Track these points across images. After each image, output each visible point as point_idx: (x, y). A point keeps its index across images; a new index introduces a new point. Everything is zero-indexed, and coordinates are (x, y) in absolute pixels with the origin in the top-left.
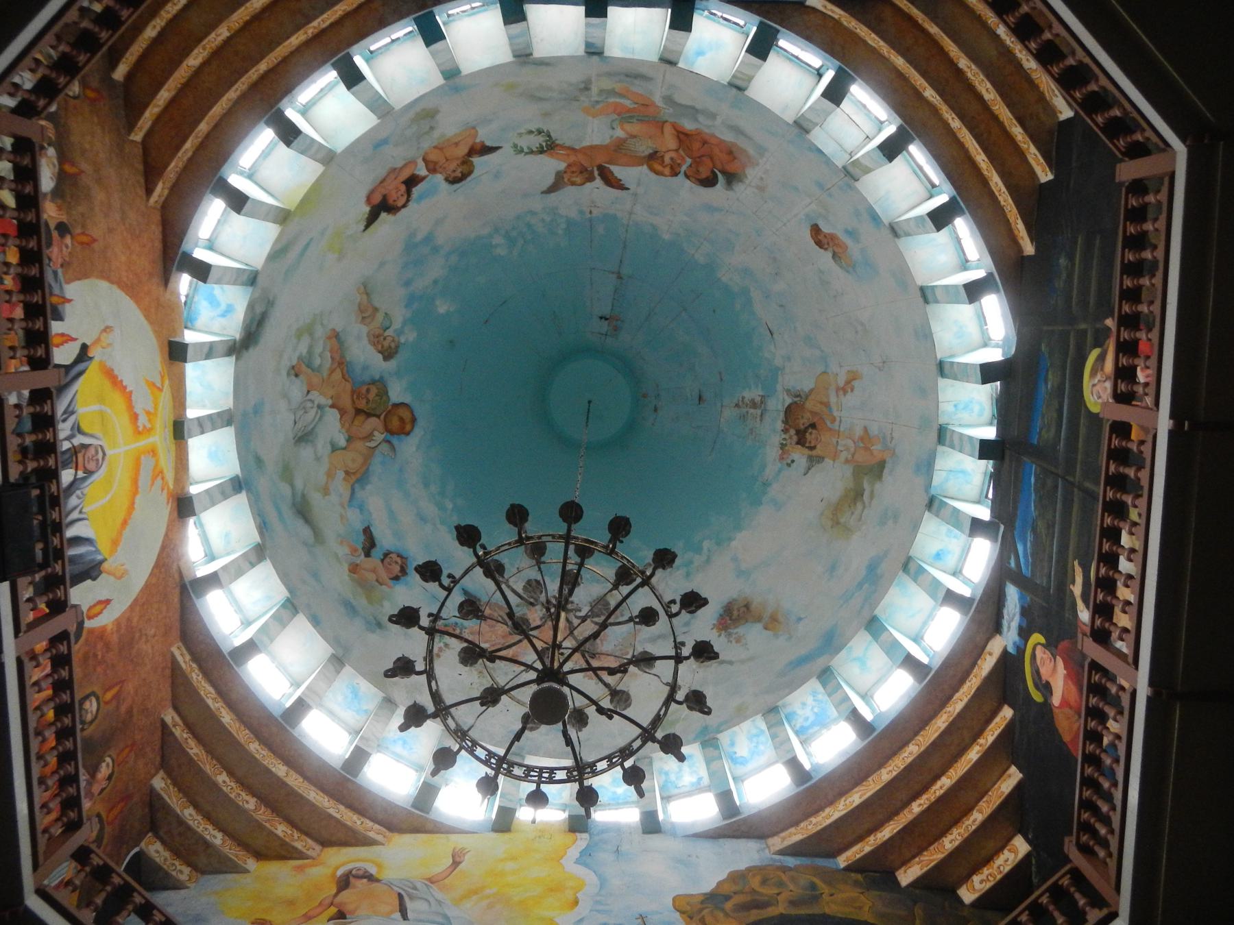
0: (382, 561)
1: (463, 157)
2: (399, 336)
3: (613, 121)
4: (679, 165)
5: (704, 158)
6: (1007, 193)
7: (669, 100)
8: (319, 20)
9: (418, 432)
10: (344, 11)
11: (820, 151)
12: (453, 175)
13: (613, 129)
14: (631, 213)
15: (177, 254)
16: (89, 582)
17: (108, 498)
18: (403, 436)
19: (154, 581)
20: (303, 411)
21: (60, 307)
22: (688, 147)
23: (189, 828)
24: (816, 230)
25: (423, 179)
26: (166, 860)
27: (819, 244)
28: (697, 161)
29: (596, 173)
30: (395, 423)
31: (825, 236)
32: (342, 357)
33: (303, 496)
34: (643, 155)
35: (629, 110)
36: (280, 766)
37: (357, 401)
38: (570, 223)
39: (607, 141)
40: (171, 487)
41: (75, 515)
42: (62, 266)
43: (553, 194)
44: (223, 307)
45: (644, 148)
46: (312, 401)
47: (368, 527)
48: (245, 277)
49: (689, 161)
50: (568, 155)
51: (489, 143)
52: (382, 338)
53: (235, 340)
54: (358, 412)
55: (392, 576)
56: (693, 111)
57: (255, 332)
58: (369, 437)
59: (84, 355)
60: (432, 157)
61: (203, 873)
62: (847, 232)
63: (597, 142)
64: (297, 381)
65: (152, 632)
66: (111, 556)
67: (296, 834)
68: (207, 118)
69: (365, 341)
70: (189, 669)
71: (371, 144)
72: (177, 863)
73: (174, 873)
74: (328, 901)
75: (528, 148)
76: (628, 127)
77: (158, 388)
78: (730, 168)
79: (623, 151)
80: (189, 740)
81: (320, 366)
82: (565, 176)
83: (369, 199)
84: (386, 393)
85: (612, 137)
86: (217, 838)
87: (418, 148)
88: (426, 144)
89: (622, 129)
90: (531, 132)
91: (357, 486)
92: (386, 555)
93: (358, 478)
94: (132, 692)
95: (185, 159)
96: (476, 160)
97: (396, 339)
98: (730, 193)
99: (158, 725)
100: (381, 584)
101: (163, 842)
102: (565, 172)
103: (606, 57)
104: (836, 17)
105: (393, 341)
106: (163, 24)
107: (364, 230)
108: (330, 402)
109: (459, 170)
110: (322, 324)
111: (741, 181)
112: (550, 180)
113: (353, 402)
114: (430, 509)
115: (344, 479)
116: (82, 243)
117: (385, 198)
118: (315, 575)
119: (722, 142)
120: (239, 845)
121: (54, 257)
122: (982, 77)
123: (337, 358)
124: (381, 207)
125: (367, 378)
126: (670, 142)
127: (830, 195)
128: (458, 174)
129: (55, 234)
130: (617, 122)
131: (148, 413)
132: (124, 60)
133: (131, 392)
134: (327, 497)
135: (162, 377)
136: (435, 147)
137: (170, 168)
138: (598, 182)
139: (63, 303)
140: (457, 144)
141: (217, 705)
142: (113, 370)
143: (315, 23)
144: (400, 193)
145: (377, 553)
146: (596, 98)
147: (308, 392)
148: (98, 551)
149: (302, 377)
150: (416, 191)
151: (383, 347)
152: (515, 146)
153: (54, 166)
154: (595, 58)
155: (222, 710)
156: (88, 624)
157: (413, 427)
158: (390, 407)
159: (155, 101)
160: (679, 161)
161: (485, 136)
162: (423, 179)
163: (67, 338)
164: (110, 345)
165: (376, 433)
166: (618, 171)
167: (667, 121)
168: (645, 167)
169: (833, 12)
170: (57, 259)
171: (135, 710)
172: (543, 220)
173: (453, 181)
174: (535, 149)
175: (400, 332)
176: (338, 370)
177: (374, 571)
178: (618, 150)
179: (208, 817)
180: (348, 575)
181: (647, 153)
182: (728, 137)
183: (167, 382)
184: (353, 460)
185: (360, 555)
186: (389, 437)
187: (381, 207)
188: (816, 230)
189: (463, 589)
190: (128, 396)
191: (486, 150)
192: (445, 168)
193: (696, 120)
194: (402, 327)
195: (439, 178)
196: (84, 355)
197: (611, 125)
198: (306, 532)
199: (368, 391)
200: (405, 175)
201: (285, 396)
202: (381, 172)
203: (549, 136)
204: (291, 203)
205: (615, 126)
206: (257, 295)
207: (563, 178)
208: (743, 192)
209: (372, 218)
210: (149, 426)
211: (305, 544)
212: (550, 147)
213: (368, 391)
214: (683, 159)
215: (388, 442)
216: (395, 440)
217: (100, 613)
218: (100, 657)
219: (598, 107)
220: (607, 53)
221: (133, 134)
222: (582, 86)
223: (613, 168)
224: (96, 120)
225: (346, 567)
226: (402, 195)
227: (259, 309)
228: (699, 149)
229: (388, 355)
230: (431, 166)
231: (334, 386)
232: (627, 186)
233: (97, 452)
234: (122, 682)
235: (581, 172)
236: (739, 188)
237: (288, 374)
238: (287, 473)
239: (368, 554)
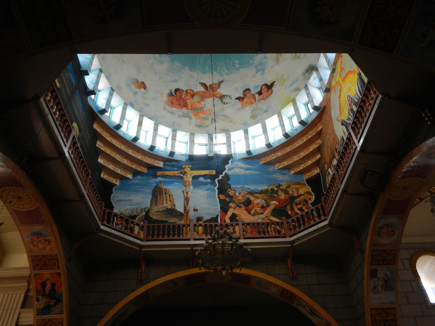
1: (245, 97)
3: (205, 107)
4: (185, 94)
5: (179, 99)
6: (105, 137)
7: (190, 118)
8: (274, 158)
11: (150, 119)
12: (248, 92)
13: (205, 105)
14: (198, 75)
15: (320, 112)
22: (184, 102)
24: (145, 88)
25: (256, 93)
27: (143, 83)
28: (181, 97)
29: (209, 88)
31: (142, 87)
34: (196, 96)
39: (206, 99)
41: (357, 96)
43: (221, 80)
45: (196, 98)
49: (183, 97)
50: (217, 94)
51: (238, 101)
56: (184, 116)
57: (310, 69)
60: (253, 100)
62: (136, 93)
63: (209, 99)
71: (268, 113)
75: (227, 97)
76: (200, 106)
78: (172, 97)
87: (257, 105)
88: (254, 105)
89: (202, 104)
90: (227, 103)
96: (242, 96)
98: (170, 89)
102: (217, 88)
103: (207, 134)
104: (156, 161)
107: (275, 81)
109: (247, 93)
111: (168, 94)
112: (222, 85)
117: (268, 91)
119: (175, 107)
122: (120, 161)
124: (269, 87)
126: (189, 102)
127: (144, 103)
130: (204, 107)
132: (317, 159)
135: (333, 88)
136: (252, 104)
138: (208, 85)
140: (247, 103)
143: (275, 157)
146: (210, 116)
150: (259, 90)
152: (231, 99)
154: (210, 134)
159: (314, 149)
160: (186, 95)
161: (239, 104)
164: (338, 116)
166: (202, 89)
167: (191, 110)
168: (195, 91)
169: (157, 163)
172: (224, 71)
173: (248, 90)
174: (226, 97)
178: (203, 97)
181: (195, 96)
182: (174, 109)
187: (269, 87)
188: (145, 88)
190: (339, 98)
191: (238, 98)
192: (251, 95)
193: (183, 112)
197: (205, 106)
200: (261, 96)
202: (267, 100)
206: (306, 81)
207: (218, 86)
208: (166, 92)
209: (272, 84)
212: (222, 97)
214: (184, 96)
220: (207, 135)
223: (204, 90)
226: (263, 89)
228: (181, 101)
230: (254, 97)
232: (200, 84)
236: (168, 91)
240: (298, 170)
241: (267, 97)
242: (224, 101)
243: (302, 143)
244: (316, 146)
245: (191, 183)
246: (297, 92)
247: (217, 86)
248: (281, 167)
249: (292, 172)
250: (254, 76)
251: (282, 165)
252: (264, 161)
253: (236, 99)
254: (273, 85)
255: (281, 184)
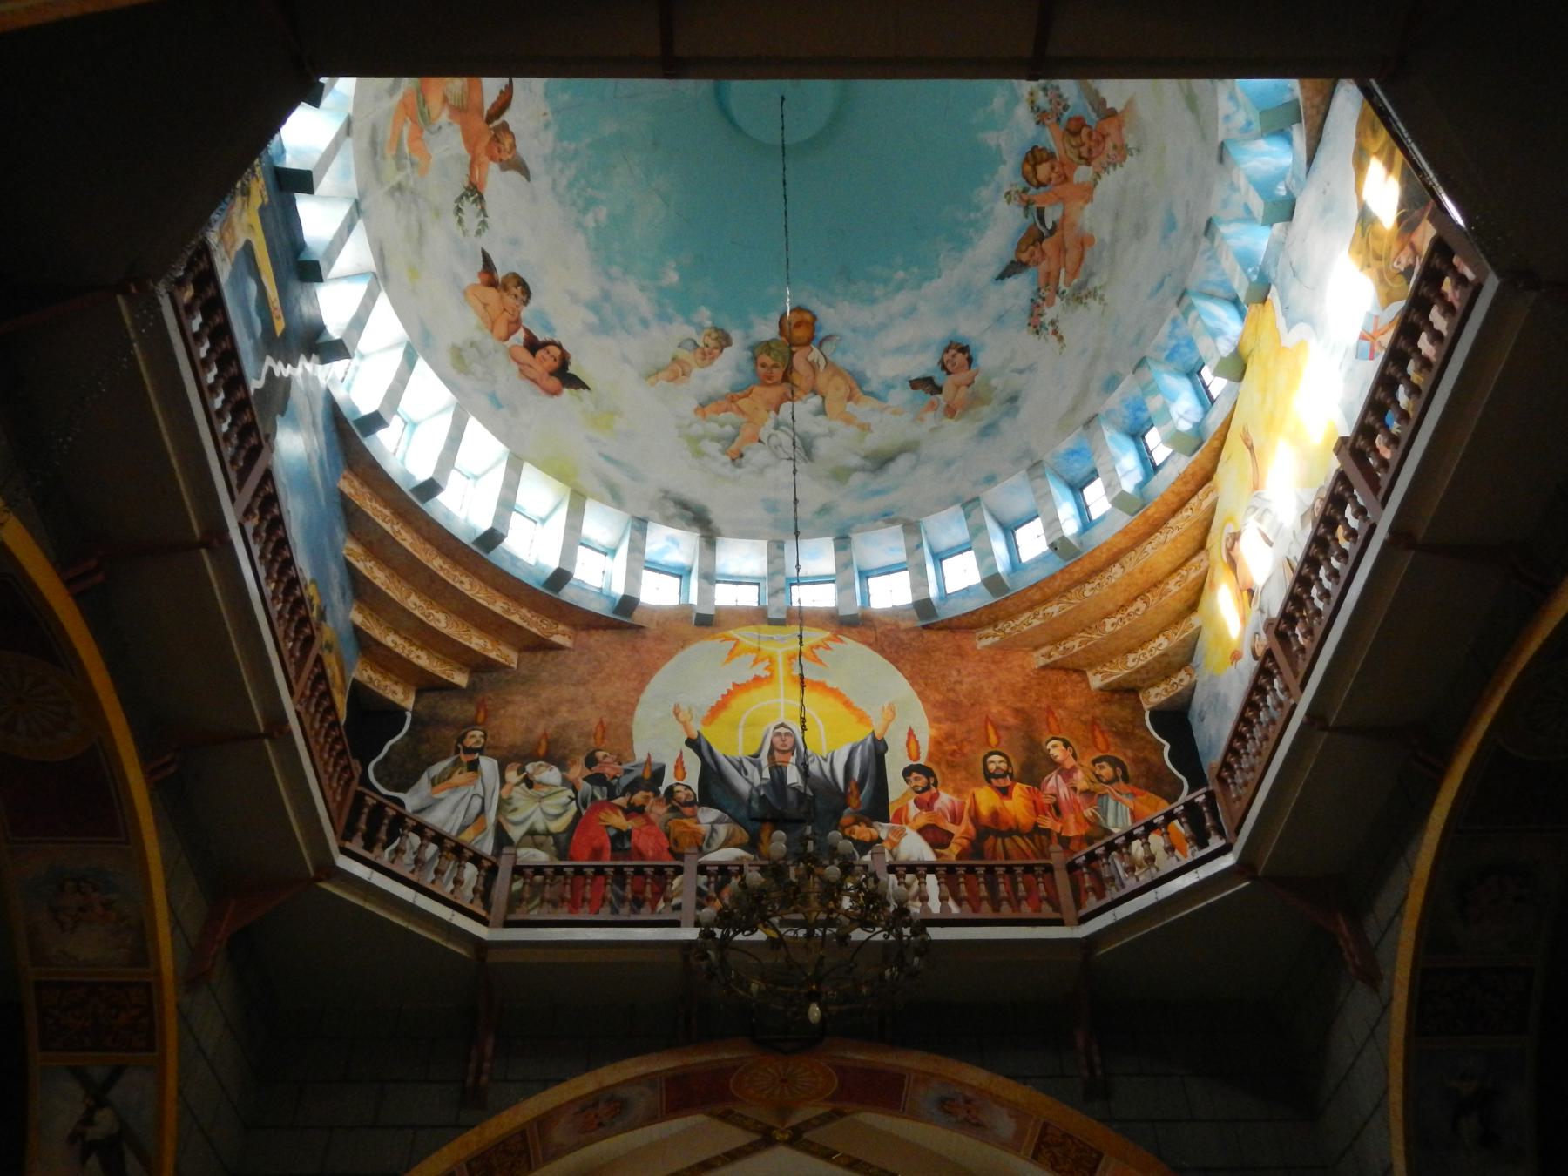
0: (949, 373)
2: (703, 328)
3: (432, 133)
9: (815, 306)
10: (371, 500)
13: (440, 128)
16: (887, 756)
17: (819, 722)
18: (817, 324)
19: (908, 667)
20: (780, 450)
21: (655, 768)
23: (1143, 667)
25: (527, 331)
26: (1166, 690)
29: (496, 123)
30: (800, 333)
32: (724, 397)
33: (866, 457)
35: (415, 122)
36: (1114, 570)
37: (775, 380)
38: (560, 137)
39: (457, 127)
40: (828, 634)
41: (826, 767)
42: (620, 764)
44: (670, 544)
46: (770, 437)
47: (910, 382)
48: (638, 535)
50: (480, 165)
52: (706, 349)
53: (702, 537)
54: (786, 378)
55: (967, 367)
57: (693, 512)
58: (813, 366)
59: (694, 744)
60: (502, 329)
61: (1190, 659)
64: (748, 455)
65: (954, 673)
66: (870, 725)
67: (1183, 572)
68: (491, 607)
69: (708, 370)
70: (1001, 634)
72: (1173, 680)
73: (1180, 688)
74: (1239, 592)
75: (478, 215)
76: (434, 113)
77: (736, 645)
79: (465, 102)
80: (1067, 645)
81: (733, 426)
82: (504, 158)
83: (554, 393)
84: (768, 342)
85: (450, 124)
86: (1162, 644)
88: (490, 343)
90: (460, 221)
91: (864, 389)
92: (944, 367)
93: (857, 385)
94: (1001, 709)
95: (529, 615)
96: (500, 274)
97: (707, 331)
99: (1043, 673)
100: (973, 382)
101: (1152, 686)
105: (709, 335)
106: (413, 648)
107: (589, 389)
108: (772, 414)
110: (690, 425)
112: (513, 175)
113: (775, 384)
114: (901, 301)
115: (856, 403)
116: (603, 738)
117: (552, 374)
118: (948, 464)
120: (1177, 623)
121: (613, 773)
123: (725, 404)
124: (564, 377)
125: (749, 367)
128: (518, 291)
129: (596, 769)
131: (756, 662)
132: (449, 679)
133: (735, 685)
134: (872, 428)
135: (727, 639)
136: (492, 331)
137: (539, 633)
138: (508, 117)
139: (650, 764)
140: (485, 305)
141: (1041, 616)
142: (712, 707)
143: (387, 527)
144: (547, 356)
145: (940, 378)
146: (409, 170)
147: (760, 441)
148: (863, 742)
149: (743, 451)
150: (542, 336)
151: (715, 348)
152: (479, 233)
153: (541, 765)
154: (363, 206)
155: (1046, 611)
156: (922, 761)
157: (809, 312)
158: (783, 339)
159: (482, 651)
161: (471, 275)
162: (527, 331)
163: (680, 765)
164: (690, 711)
165: (810, 358)
170: (614, 769)
171: (1019, 705)
172: (562, 171)
173: (527, 292)
174: (479, 207)
175: (700, 327)
176: (740, 402)
177: (958, 387)
179: (1143, 643)
180: (958, 419)
183: (732, 633)
184: (837, 389)
185: (939, 400)
186: (816, 342)
187: (564, 377)
189: (997, 279)
190: (739, 688)
194: (694, 324)
195: (525, 313)
196: (694, 744)
197: (436, 132)
198: (903, 463)
199: (763, 365)
200: (525, 356)
201: (761, 471)
202: (526, 386)
203: (461, 198)
204: (565, 491)
205: (436, 127)
207: (508, 160)
209: (575, 382)
210: (767, 663)
211: (914, 468)
212: (474, 191)
213: (763, 365)
215: (820, 345)
216: (821, 334)
217: (917, 742)
218: (955, 747)
219: (416, 158)
220: (357, 196)
221: (512, 665)
222: (397, 194)
223: (488, 105)
224: (502, 712)
225: (947, 421)
227: (672, 509)
229: (724, 340)
231: (757, 409)
233: (779, 734)
234: (987, 718)
235: (498, 141)
237: (739, 466)
238: (840, 475)
239: (938, 390)
240: (376, 631)
241: (534, 381)
242: (464, 209)
243: (485, 604)
244: (493, 655)
245: (233, 254)
246: (608, 497)
247: (507, 157)
248: (360, 566)
249: (357, 618)
250: (574, 297)
251: (366, 567)
252: (352, 491)
253: (484, 253)
254: (576, 388)
255: (328, 616)
